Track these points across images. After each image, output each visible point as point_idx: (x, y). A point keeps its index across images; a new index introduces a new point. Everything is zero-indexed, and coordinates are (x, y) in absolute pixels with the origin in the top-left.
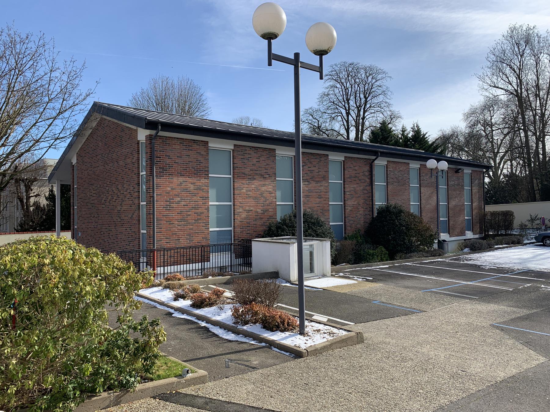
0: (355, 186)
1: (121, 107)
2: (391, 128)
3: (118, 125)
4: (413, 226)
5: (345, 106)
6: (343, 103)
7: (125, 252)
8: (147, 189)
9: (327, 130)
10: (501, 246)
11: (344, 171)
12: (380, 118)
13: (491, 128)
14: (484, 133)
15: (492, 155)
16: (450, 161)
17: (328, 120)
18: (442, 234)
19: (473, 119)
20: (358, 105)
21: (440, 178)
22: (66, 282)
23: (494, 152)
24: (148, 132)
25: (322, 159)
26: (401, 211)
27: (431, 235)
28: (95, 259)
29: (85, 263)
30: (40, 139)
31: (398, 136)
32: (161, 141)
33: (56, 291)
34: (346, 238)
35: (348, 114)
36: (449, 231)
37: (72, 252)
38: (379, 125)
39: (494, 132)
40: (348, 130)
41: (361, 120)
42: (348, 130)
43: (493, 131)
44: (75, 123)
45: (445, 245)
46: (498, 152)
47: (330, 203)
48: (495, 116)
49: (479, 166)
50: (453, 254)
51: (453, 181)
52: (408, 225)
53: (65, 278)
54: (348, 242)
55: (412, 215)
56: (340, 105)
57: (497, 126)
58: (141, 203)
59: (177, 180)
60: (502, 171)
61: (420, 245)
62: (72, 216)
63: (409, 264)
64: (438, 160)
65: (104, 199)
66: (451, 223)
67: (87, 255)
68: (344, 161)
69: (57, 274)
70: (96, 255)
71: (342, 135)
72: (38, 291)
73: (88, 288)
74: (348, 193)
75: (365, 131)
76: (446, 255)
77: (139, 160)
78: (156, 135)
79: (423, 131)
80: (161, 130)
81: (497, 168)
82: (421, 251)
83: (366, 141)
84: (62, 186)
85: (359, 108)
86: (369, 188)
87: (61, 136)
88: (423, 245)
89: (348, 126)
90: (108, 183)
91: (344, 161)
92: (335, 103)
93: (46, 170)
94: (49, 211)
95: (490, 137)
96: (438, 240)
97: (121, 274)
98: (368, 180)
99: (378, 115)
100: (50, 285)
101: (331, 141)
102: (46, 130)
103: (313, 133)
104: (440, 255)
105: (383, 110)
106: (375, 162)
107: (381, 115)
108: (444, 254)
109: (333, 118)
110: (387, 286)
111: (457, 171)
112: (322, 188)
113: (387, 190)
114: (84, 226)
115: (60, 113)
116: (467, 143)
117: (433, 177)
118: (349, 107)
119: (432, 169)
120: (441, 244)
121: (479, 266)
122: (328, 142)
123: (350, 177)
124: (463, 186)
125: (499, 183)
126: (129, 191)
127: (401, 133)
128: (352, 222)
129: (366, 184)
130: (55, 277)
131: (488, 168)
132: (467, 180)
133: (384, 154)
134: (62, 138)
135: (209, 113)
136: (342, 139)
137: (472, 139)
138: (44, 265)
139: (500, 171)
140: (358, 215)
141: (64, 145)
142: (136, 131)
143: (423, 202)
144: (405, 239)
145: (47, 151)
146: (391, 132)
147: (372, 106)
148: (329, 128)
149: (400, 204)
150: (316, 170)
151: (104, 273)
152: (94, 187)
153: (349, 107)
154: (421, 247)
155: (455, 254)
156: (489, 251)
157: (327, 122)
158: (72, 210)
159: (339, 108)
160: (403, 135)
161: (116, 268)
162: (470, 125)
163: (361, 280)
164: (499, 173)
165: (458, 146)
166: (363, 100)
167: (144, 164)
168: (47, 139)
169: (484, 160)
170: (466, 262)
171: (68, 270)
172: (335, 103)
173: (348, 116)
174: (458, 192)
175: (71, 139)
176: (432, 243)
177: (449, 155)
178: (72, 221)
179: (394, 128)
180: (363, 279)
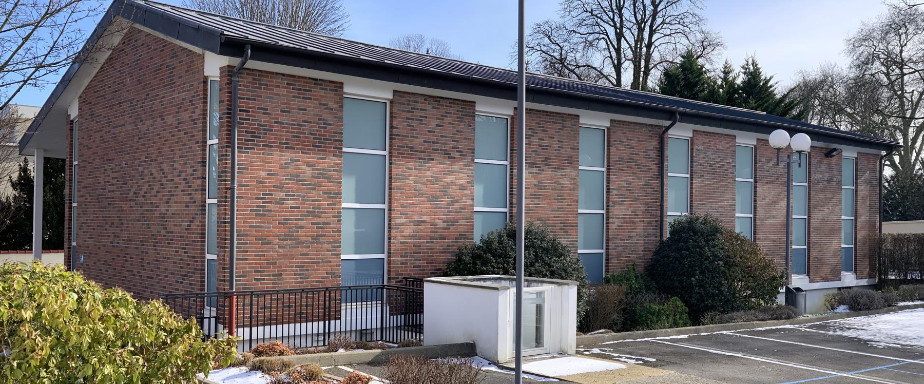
0: (630, 179)
1: (173, 7)
2: (702, 67)
3: (166, 44)
4: (738, 260)
5: (613, 20)
6: (611, 14)
7: (175, 297)
8: (221, 173)
9: (578, 67)
10: (911, 303)
11: (609, 149)
12: (682, 45)
13: (901, 69)
14: (885, 79)
15: (899, 123)
16: (815, 134)
17: (580, 47)
18: (794, 277)
19: (865, 50)
20: (639, 18)
21: (794, 167)
22: (62, 356)
23: (904, 118)
24: (225, 61)
25: (568, 124)
26: (716, 230)
27: (774, 278)
28: (122, 311)
29: (102, 319)
30: (6, 64)
31: (715, 83)
32: (250, 79)
33: (43, 374)
34: (607, 281)
35: (620, 36)
36: (808, 271)
37: (76, 297)
38: (679, 60)
39: (906, 77)
40: (618, 68)
41: (644, 49)
42: (618, 68)
43: (903, 75)
44: (78, 36)
45: (800, 298)
46: (912, 118)
47: (580, 211)
48: (909, 45)
49: (873, 144)
50: (814, 317)
51: (820, 173)
52: (728, 256)
53: (63, 348)
54: (613, 288)
55: (737, 237)
56: (605, 17)
57: (912, 65)
58: (208, 201)
59: (278, 157)
60: (918, 154)
61: (751, 296)
62: (66, 222)
63: (728, 333)
64: (792, 132)
65: (133, 190)
66: (814, 254)
67: (106, 303)
68: (609, 129)
69: (46, 340)
70: (124, 303)
71: (606, 77)
72: (8, 373)
73: (108, 370)
74: (615, 192)
75: (653, 71)
76: (801, 318)
77: (205, 114)
78: (242, 68)
79: (765, 73)
80: (251, 58)
81: (909, 149)
82: (753, 308)
83: (654, 90)
84: (47, 160)
85: (640, 24)
86: (655, 183)
87: (50, 60)
88: (756, 297)
89: (619, 59)
90: (143, 158)
91: (609, 129)
92: (595, 13)
93: (13, 127)
94: (18, 209)
95: (897, 87)
96: (787, 289)
97: (174, 341)
98: (654, 167)
99: (677, 40)
100: (33, 363)
101: (585, 88)
102: (19, 48)
103: (551, 71)
104: (788, 318)
105: (687, 30)
106: (670, 132)
107: (684, 40)
108: (796, 315)
109: (591, 44)
110: (684, 376)
111: (829, 154)
112: (565, 181)
113: (691, 188)
114: (91, 242)
115: (48, 14)
116: (852, 98)
117: (782, 165)
118: (622, 21)
119: (779, 149)
120: (793, 295)
121: (866, 342)
122: (578, 89)
123: (620, 161)
124: (839, 183)
125: (912, 179)
126: (183, 176)
127: (722, 75)
128: (620, 249)
129: (650, 174)
130: (43, 346)
131: (891, 148)
132: (847, 171)
133: (687, 118)
134: (49, 65)
135: (345, 25)
136: (607, 84)
137: (863, 90)
138: (22, 321)
139: (914, 154)
140: (633, 234)
141: (55, 78)
142: (202, 57)
143: (760, 211)
144: (722, 285)
145: (18, 91)
146: (701, 74)
147: (667, 21)
148: (581, 63)
149: (715, 215)
150: (554, 144)
151: (141, 340)
152: (113, 166)
153: (622, 21)
154: (753, 300)
155: (819, 316)
156: (886, 312)
157: (577, 51)
158: (67, 210)
159: (602, 23)
160: (725, 79)
161: (165, 330)
162: (858, 62)
163: (633, 361)
164: (913, 158)
165: (834, 103)
166: (650, 9)
167: (216, 123)
168: (20, 66)
169: (883, 131)
170: (839, 333)
171: (68, 333)
172: (595, 13)
173: (619, 41)
174: (829, 196)
175: (67, 68)
176: (774, 293)
177: (815, 122)
178: (66, 231)
179: (708, 66)
180: (637, 360)
